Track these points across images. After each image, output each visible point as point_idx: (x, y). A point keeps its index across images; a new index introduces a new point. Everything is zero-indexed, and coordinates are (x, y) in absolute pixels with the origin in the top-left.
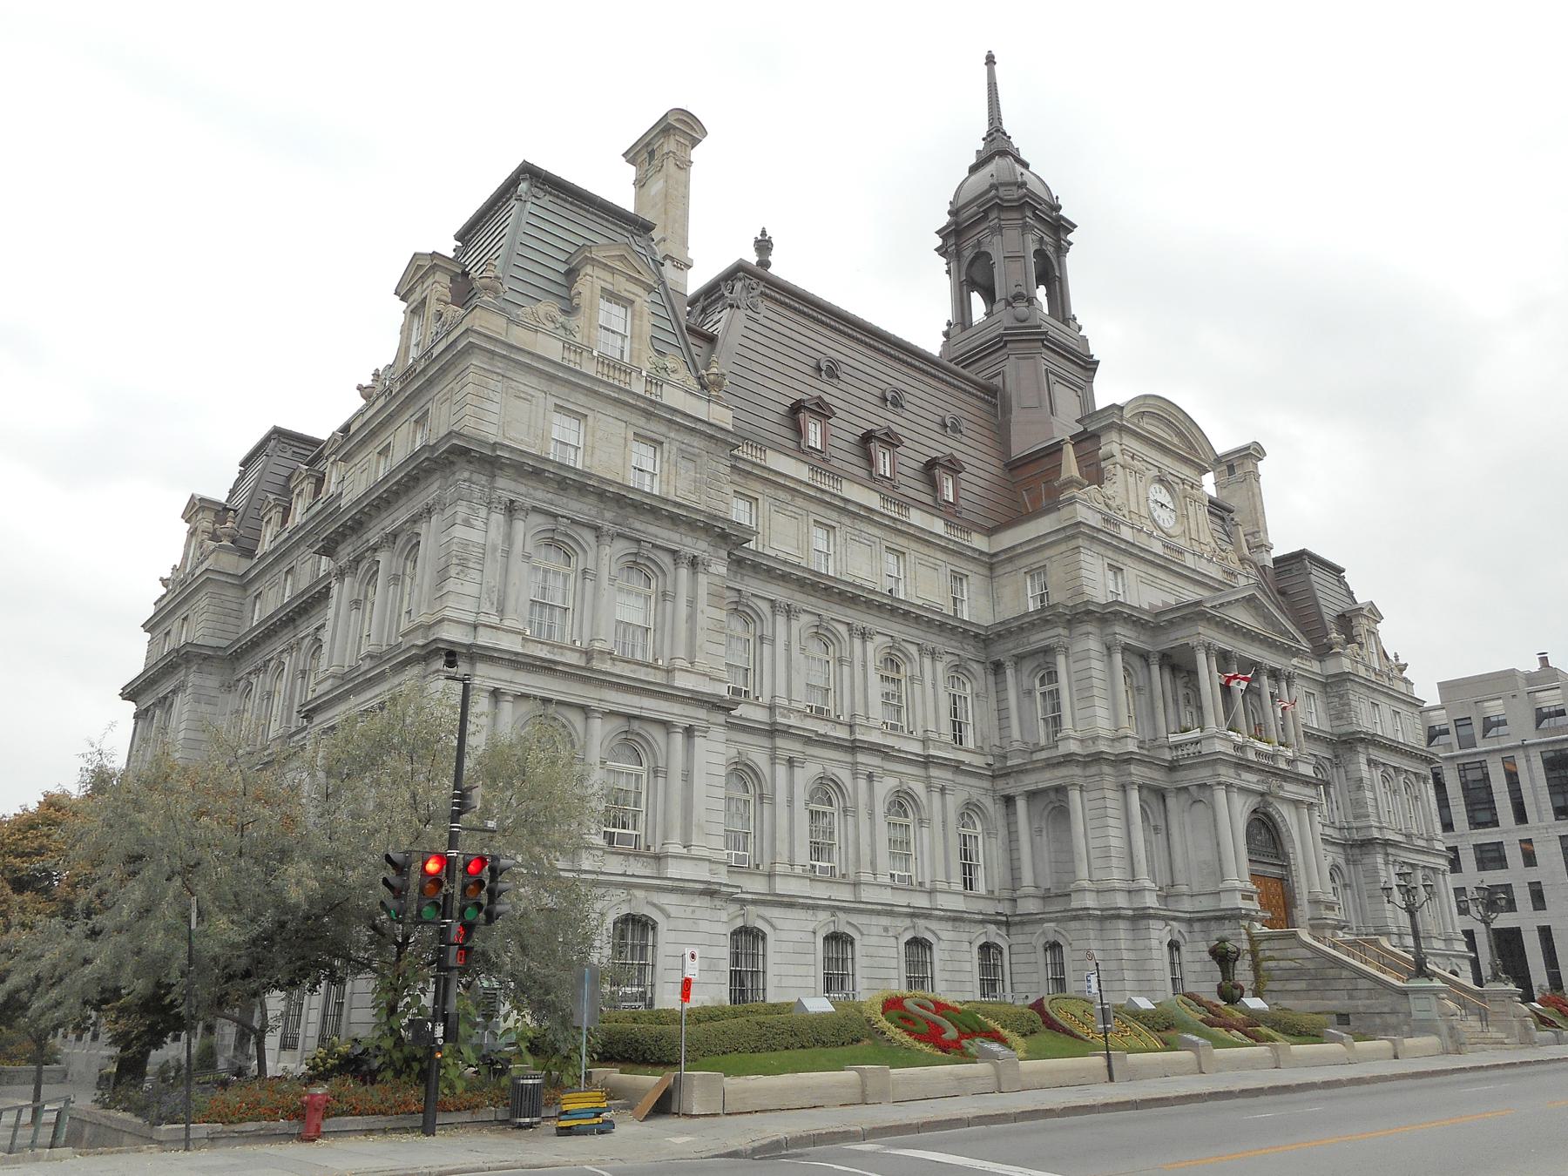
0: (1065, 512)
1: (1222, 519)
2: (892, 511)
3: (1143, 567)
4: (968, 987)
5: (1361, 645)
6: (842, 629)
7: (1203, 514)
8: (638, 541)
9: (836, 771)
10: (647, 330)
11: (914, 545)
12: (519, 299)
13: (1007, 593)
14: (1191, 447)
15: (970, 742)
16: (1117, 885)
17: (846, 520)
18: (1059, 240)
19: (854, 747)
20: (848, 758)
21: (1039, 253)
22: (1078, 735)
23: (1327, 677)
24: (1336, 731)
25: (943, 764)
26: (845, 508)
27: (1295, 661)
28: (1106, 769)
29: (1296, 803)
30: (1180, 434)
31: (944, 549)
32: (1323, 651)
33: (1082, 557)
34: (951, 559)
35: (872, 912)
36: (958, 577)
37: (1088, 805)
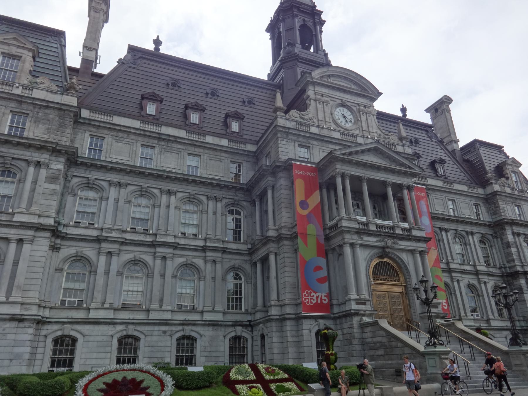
1: (427, 131)
2: (194, 137)
4: (221, 359)
5: (507, 178)
6: (156, 191)
7: (373, 120)
8: (3, 157)
9: (141, 256)
11: (207, 151)
14: (363, 89)
15: (242, 240)
16: (287, 302)
17: (163, 143)
18: (314, 19)
19: (153, 245)
20: (152, 250)
21: (304, 27)
22: (277, 227)
23: (487, 195)
24: (494, 220)
25: (214, 249)
26: (160, 137)
27: (415, 180)
28: (286, 242)
29: (412, 252)
30: (355, 83)
32: (484, 183)
33: (279, 142)
35: (154, 324)
37: (279, 262)
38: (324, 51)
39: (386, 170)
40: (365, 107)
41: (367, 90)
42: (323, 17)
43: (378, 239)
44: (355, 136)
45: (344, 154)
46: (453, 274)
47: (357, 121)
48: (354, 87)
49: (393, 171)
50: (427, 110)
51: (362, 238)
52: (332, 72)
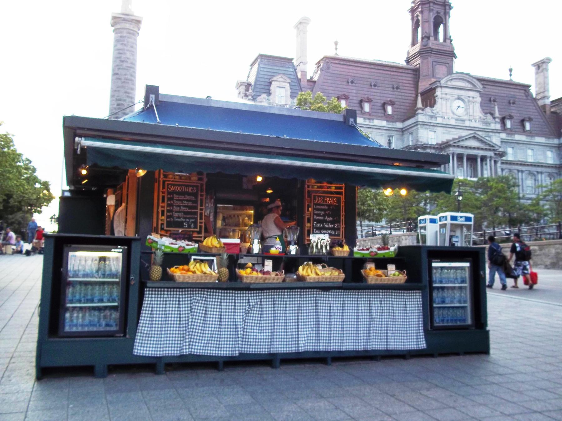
0: (416, 118)
1: (525, 90)
2: (368, 122)
3: (445, 129)
10: (289, 94)
12: (258, 94)
13: (406, 139)
18: (445, 10)
23: (559, 144)
30: (469, 82)
31: (385, 130)
34: (388, 132)
36: (389, 136)
38: (450, 37)
39: (478, 149)
40: (473, 98)
42: (452, 5)
44: (464, 121)
45: (455, 143)
47: (467, 109)
49: (482, 149)
50: (534, 65)
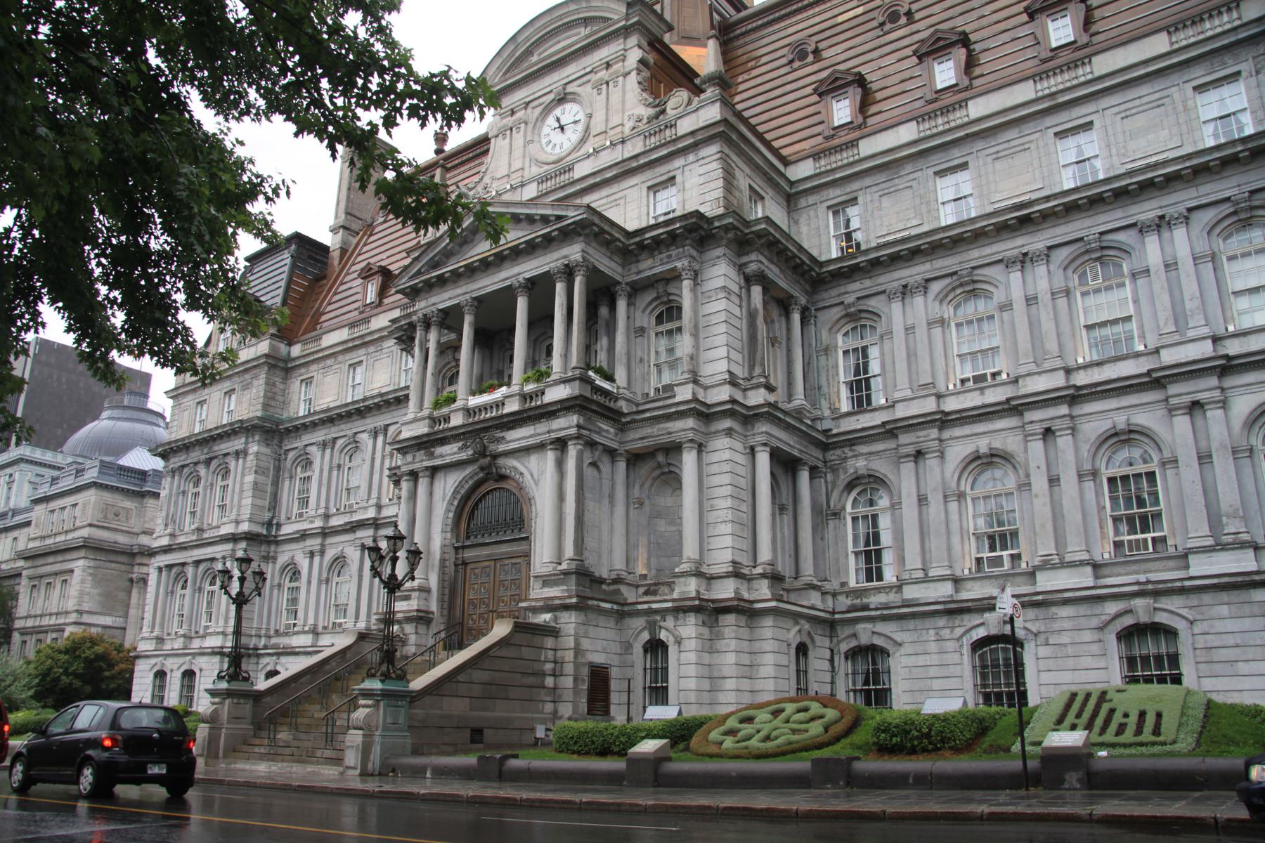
17: (371, 349)
30: (586, 21)
41: (606, 19)
43: (460, 444)
45: (419, 273)
46: (1030, 416)
48: (583, 31)
51: (432, 454)
52: (527, 39)
